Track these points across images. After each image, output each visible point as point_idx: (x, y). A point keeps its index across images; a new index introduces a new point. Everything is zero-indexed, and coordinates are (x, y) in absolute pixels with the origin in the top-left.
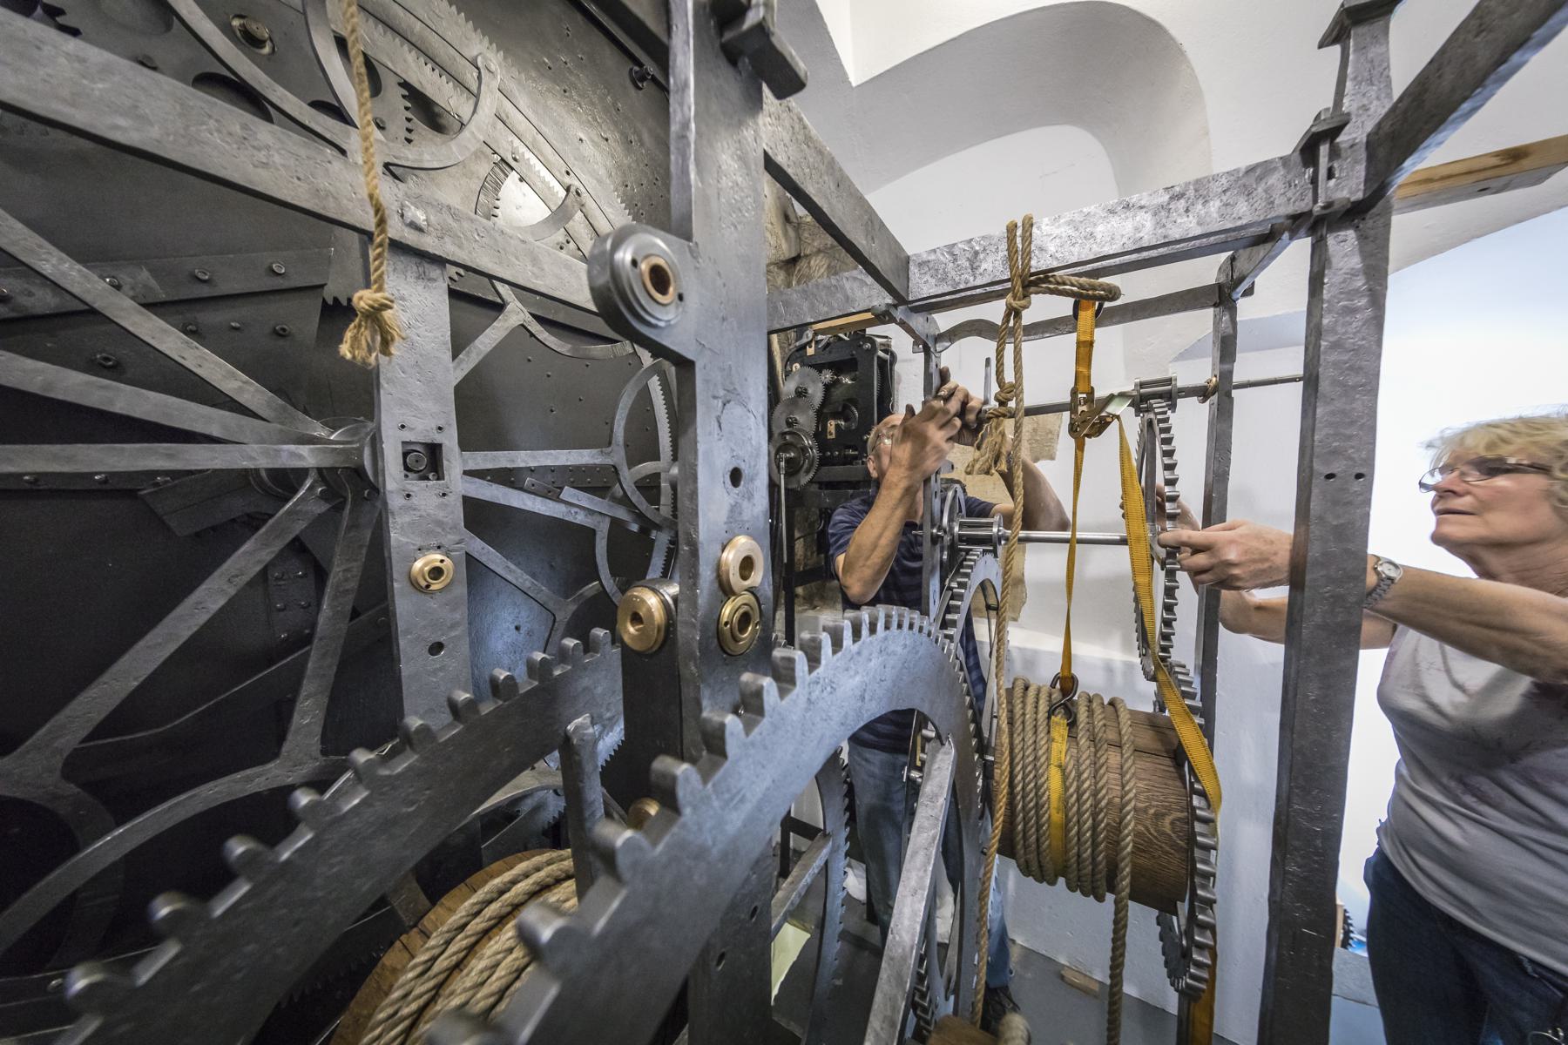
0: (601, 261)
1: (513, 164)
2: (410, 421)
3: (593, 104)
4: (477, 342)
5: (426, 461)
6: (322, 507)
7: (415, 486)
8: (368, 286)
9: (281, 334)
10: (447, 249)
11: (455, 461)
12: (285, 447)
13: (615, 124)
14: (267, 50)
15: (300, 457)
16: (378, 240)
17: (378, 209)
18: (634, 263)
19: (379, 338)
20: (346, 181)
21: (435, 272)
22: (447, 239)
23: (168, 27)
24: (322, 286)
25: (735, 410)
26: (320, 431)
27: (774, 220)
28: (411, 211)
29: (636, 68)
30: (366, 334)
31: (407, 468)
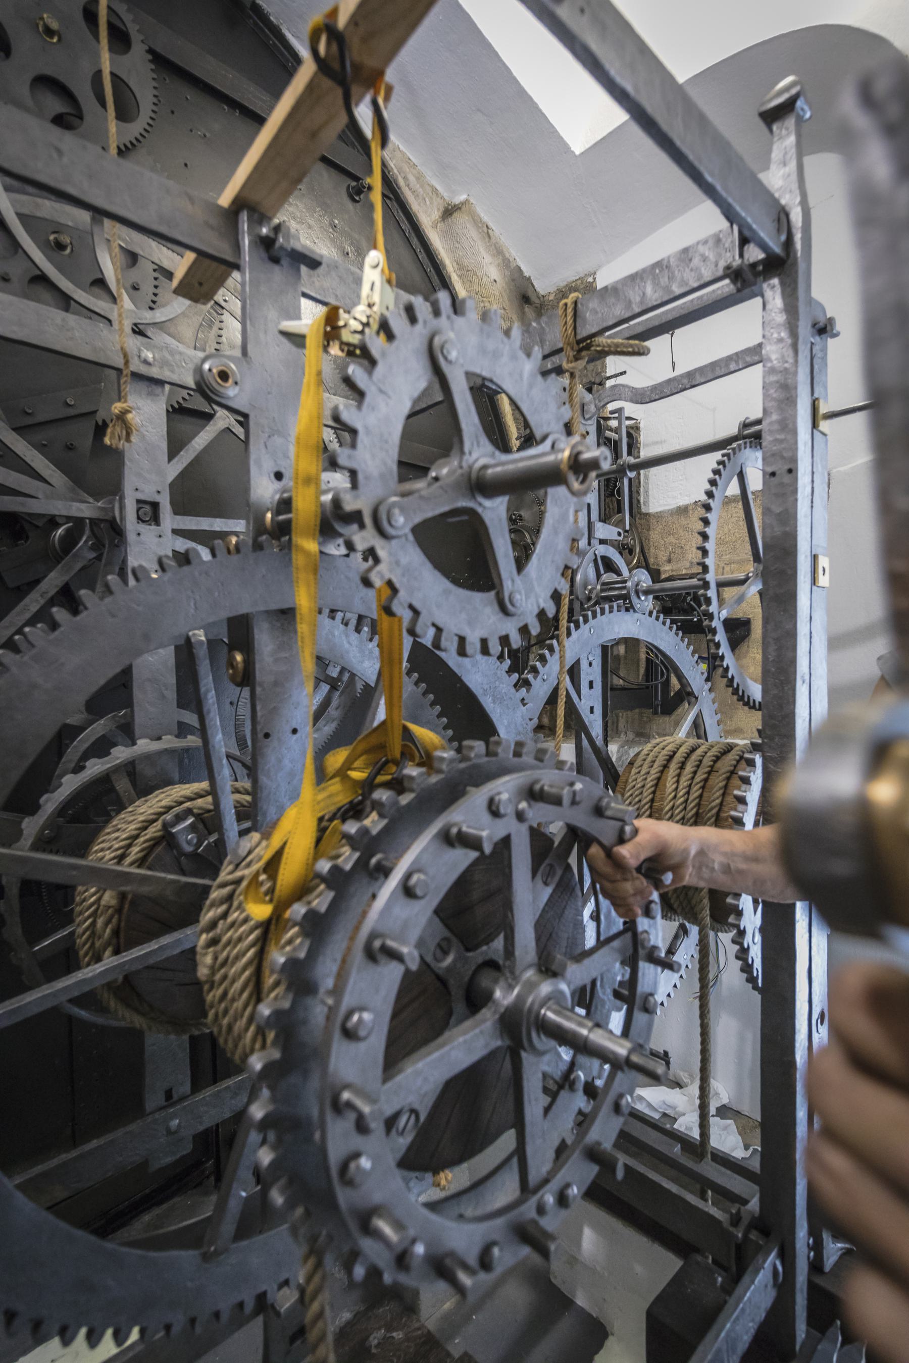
1: (223, 304)
4: (193, 442)
5: (150, 512)
6: (93, 555)
7: (143, 528)
8: (119, 400)
10: (166, 374)
11: (169, 521)
12: (75, 504)
14: (68, 251)
15: (81, 510)
16: (125, 373)
17: (125, 356)
19: (124, 433)
20: (110, 343)
21: (158, 390)
22: (165, 369)
23: (16, 252)
26: (91, 500)
28: (147, 355)
30: (118, 429)
31: (139, 518)
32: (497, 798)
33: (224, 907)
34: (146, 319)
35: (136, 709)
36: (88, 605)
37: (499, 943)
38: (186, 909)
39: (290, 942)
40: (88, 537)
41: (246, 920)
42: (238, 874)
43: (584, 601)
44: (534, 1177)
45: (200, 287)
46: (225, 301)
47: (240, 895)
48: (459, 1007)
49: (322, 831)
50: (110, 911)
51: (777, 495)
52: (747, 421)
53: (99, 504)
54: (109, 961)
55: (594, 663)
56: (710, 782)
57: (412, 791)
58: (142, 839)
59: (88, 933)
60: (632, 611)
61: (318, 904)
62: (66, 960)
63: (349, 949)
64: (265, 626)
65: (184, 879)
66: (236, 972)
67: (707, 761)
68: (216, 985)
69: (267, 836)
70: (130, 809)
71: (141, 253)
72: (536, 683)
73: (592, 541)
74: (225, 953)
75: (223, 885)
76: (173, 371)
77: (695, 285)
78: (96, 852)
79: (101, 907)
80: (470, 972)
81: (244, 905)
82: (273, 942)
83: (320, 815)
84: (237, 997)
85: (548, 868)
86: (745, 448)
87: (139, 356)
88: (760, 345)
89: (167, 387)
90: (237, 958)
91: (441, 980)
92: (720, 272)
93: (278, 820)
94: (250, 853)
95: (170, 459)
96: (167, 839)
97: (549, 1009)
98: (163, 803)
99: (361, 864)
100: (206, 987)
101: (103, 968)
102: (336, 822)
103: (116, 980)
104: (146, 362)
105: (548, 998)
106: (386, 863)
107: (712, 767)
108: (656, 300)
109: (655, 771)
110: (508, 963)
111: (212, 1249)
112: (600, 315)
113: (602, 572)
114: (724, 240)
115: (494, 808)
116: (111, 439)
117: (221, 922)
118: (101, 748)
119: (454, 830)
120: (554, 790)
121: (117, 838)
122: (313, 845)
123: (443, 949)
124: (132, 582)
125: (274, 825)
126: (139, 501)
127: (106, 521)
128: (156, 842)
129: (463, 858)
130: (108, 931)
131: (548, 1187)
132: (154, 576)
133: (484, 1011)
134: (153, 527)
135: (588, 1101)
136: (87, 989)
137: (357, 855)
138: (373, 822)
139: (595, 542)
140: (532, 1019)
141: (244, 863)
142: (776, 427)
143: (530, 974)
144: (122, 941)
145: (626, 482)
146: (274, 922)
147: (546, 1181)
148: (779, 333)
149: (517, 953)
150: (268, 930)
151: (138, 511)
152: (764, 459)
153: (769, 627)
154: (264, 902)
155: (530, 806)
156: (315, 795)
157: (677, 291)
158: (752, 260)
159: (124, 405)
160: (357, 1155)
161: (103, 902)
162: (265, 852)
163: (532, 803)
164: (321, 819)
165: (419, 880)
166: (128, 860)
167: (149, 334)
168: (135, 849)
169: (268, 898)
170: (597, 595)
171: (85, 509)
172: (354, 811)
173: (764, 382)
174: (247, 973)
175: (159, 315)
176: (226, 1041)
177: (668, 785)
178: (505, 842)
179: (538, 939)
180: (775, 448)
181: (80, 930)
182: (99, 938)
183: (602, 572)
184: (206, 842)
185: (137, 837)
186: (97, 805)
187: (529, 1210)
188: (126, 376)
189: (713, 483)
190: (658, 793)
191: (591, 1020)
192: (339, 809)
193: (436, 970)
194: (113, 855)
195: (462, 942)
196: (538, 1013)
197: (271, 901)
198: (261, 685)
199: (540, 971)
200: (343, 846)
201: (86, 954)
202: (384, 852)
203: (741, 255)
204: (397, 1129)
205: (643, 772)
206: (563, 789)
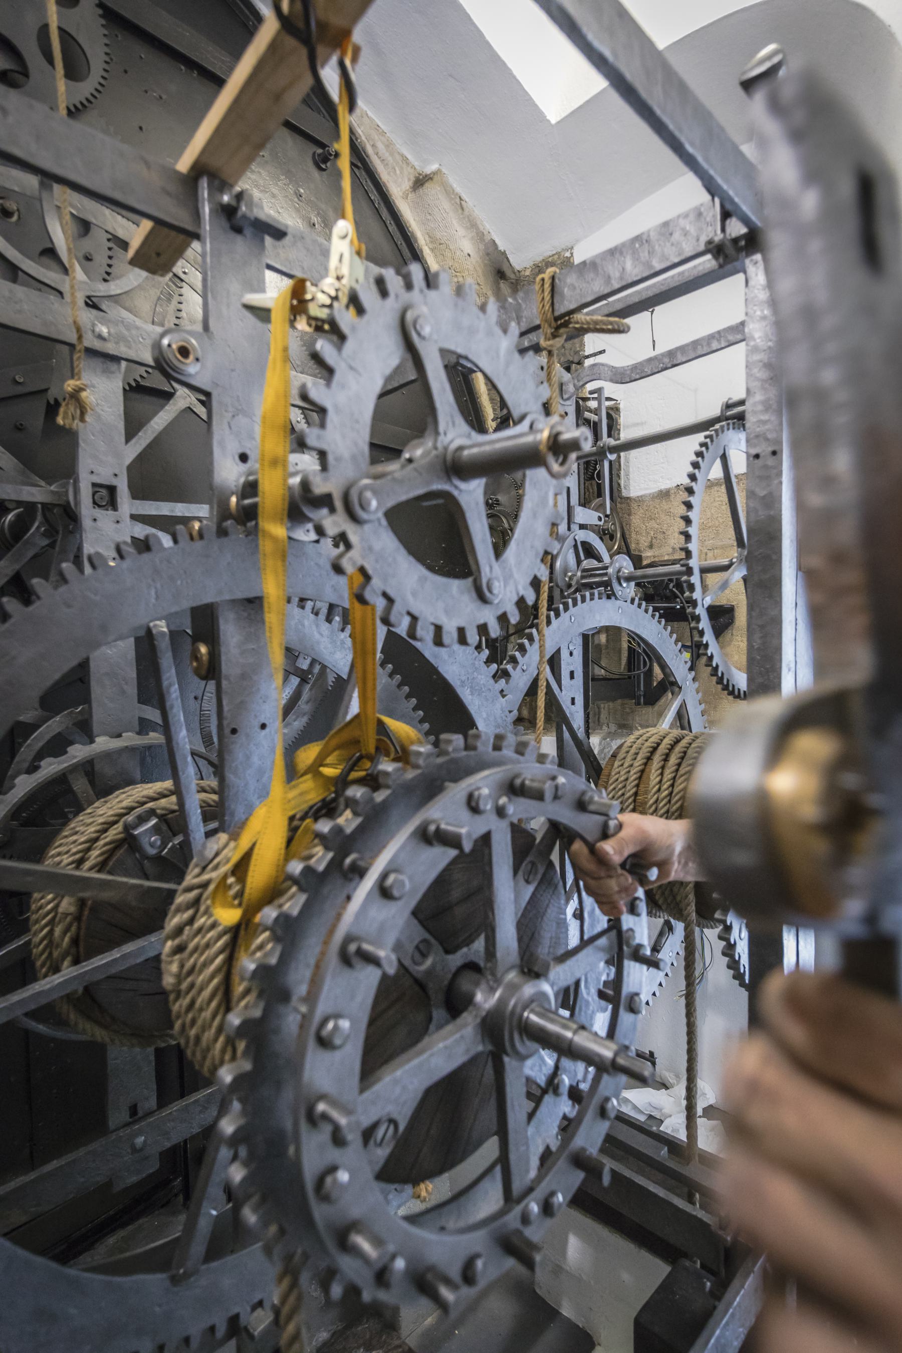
0: (157, 346)
1: (183, 276)
2: (98, 469)
3: (274, 196)
4: (152, 422)
5: (107, 497)
6: (45, 542)
8: (72, 377)
9: (19, 428)
10: (121, 350)
11: (127, 505)
13: (297, 210)
14: (15, 218)
15: (32, 494)
16: (78, 348)
17: (78, 330)
18: (169, 345)
19: (78, 412)
21: (113, 367)
22: (122, 344)
24: (46, 390)
25: (242, 420)
26: (43, 483)
27: (481, 280)
28: (101, 329)
29: (320, 151)
30: (72, 408)
31: (95, 503)
32: (476, 793)
33: (190, 912)
34: (100, 291)
35: (94, 705)
36: (42, 595)
37: (479, 944)
38: (150, 916)
39: (261, 947)
40: (40, 523)
41: (214, 925)
42: (205, 877)
44: (517, 1186)
45: (158, 257)
46: (185, 273)
47: (207, 899)
48: (438, 1014)
49: (293, 830)
50: (69, 919)
51: (761, 478)
53: (52, 488)
54: (68, 972)
57: (388, 787)
58: (101, 843)
59: (45, 942)
61: (290, 907)
62: (23, 971)
63: (323, 953)
64: (231, 616)
65: (147, 884)
66: (203, 981)
68: (183, 993)
69: (235, 836)
70: (89, 811)
71: (93, 220)
72: (515, 674)
74: (192, 960)
75: (189, 889)
76: (130, 348)
77: (676, 260)
78: (53, 856)
79: (59, 915)
80: (449, 976)
81: (211, 909)
82: (243, 948)
83: (291, 813)
84: (205, 1006)
85: (530, 866)
87: (93, 331)
88: (743, 324)
89: (124, 364)
90: (205, 965)
91: (420, 984)
92: (702, 247)
93: (247, 819)
94: (217, 854)
95: (128, 440)
96: (129, 841)
97: (532, 1011)
98: (124, 804)
99: (335, 865)
100: (172, 997)
101: (61, 980)
102: (308, 821)
103: (76, 991)
104: (100, 337)
105: (532, 1001)
106: (361, 863)
110: (489, 965)
111: (181, 1271)
112: (578, 291)
114: (705, 214)
115: (473, 804)
116: (64, 418)
117: (187, 928)
118: (57, 746)
119: (432, 828)
120: (535, 785)
121: (75, 842)
122: (284, 845)
123: (422, 951)
124: (88, 569)
125: (243, 824)
126: (94, 485)
127: (58, 505)
128: (117, 845)
129: (443, 856)
130: (67, 939)
131: (533, 1195)
132: (112, 564)
133: (465, 1015)
134: (110, 512)
135: (573, 1106)
136: (44, 1001)
137: (330, 855)
138: (347, 820)
140: (515, 1023)
141: (211, 866)
142: (760, 407)
143: (512, 976)
144: (81, 949)
146: (243, 926)
147: (530, 1190)
148: (762, 311)
149: (499, 954)
150: (237, 935)
151: (93, 495)
152: (748, 441)
153: (754, 614)
154: (232, 906)
155: (510, 800)
156: (286, 793)
157: (658, 266)
158: (734, 235)
159: (78, 383)
160: (333, 1169)
161: (60, 910)
162: (234, 854)
163: (513, 798)
164: (292, 819)
165: (395, 881)
166: (87, 865)
167: (104, 307)
168: (95, 853)
169: (236, 902)
171: (37, 493)
172: (327, 809)
173: (747, 362)
174: (215, 981)
175: (114, 288)
176: (194, 1053)
178: (485, 840)
179: (520, 940)
180: (758, 429)
181: (37, 939)
182: (58, 946)
184: (170, 845)
185: (96, 840)
186: (54, 806)
187: (512, 1219)
188: (80, 351)
189: (696, 465)
191: (575, 1022)
192: (311, 808)
193: (415, 974)
194: (71, 859)
195: (441, 944)
196: (521, 1016)
197: (240, 905)
198: (227, 678)
199: (523, 972)
200: (315, 846)
201: (43, 965)
202: (359, 852)
203: (723, 230)
204: (375, 1141)
206: (544, 783)
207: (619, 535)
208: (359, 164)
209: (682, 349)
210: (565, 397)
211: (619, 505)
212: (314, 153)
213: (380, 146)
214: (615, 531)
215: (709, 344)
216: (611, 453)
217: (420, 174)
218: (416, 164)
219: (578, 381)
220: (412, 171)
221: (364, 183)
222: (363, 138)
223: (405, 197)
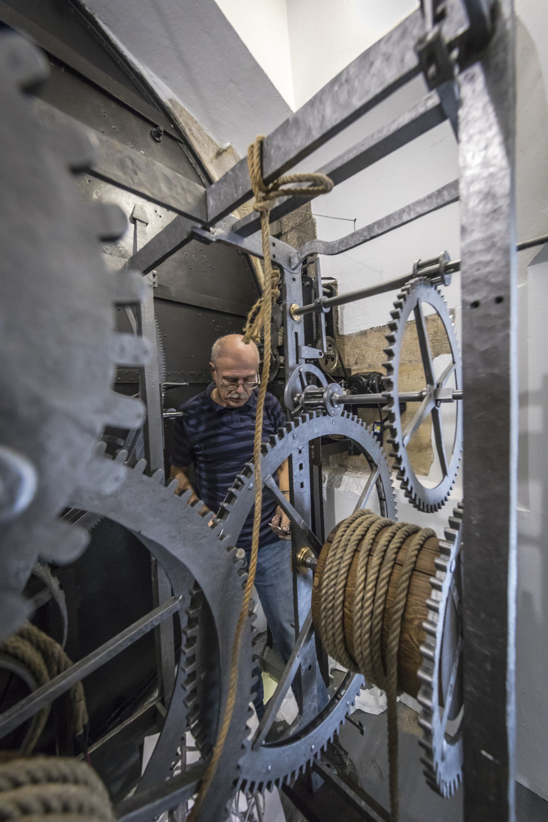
29: (155, 130)
43: (291, 409)
51: (481, 329)
52: (420, 263)
55: (303, 451)
56: (395, 577)
60: (328, 415)
67: (390, 555)
73: (299, 360)
86: (421, 284)
107: (395, 559)
108: (336, 120)
109: (347, 556)
112: (283, 150)
113: (306, 384)
139: (302, 361)
145: (323, 316)
170: (302, 402)
177: (359, 574)
183: (306, 384)
190: (350, 578)
205: (338, 556)
207: (337, 358)
208: (182, 141)
209: (379, 223)
210: (293, 267)
211: (337, 340)
212: (151, 131)
213: (194, 129)
214: (335, 356)
215: (400, 217)
216: (326, 307)
217: (220, 149)
218: (218, 143)
219: (301, 255)
220: (215, 147)
221: (186, 152)
222: (183, 124)
223: (211, 162)
